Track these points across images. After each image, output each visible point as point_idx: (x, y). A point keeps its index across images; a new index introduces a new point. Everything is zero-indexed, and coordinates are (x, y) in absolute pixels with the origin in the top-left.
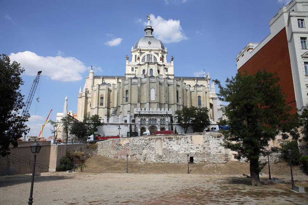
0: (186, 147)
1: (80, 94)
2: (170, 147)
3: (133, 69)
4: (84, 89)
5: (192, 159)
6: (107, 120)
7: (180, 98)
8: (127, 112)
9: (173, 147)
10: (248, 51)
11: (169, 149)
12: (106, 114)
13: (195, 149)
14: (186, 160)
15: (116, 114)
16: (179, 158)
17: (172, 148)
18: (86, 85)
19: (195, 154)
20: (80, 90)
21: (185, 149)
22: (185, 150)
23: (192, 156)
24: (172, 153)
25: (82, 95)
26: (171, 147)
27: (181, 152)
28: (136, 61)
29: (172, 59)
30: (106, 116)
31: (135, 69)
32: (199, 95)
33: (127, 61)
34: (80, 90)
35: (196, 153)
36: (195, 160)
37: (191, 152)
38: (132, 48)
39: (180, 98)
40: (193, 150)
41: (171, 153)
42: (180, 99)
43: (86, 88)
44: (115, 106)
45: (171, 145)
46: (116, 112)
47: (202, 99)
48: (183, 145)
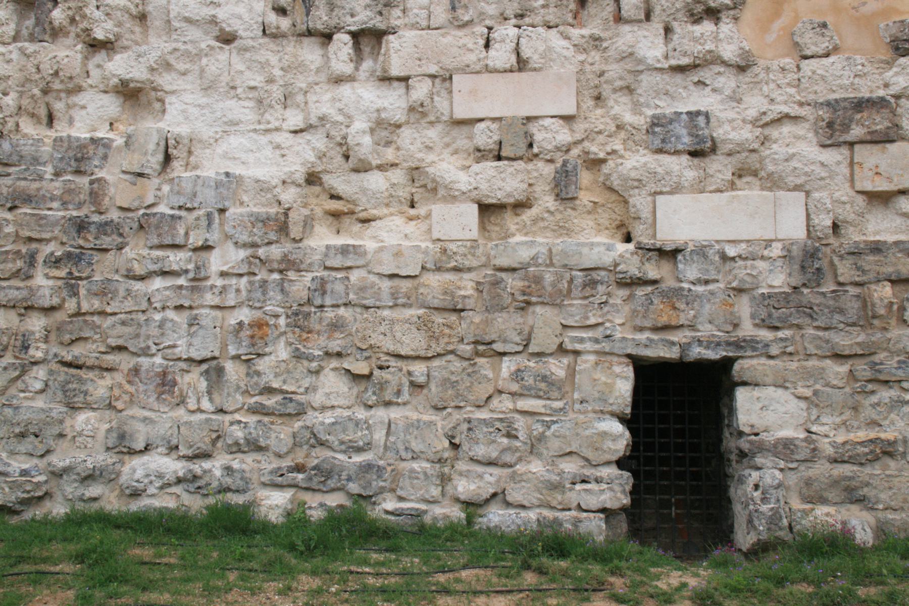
0: (547, 97)
2: (91, 116)
5: (681, 418)
9: (183, 113)
11: (79, 157)
13: (799, 148)
14: (573, 460)
16: (332, 386)
17: (151, 128)
19: (778, 280)
21: (512, 144)
22: (504, 181)
23: (696, 338)
24: (137, 254)
26: (131, 94)
27: (393, 238)
35: (809, 260)
36: (785, 449)
37: (682, 219)
40: (719, 168)
41: (104, 268)
45: (119, 66)
48: (461, 46)
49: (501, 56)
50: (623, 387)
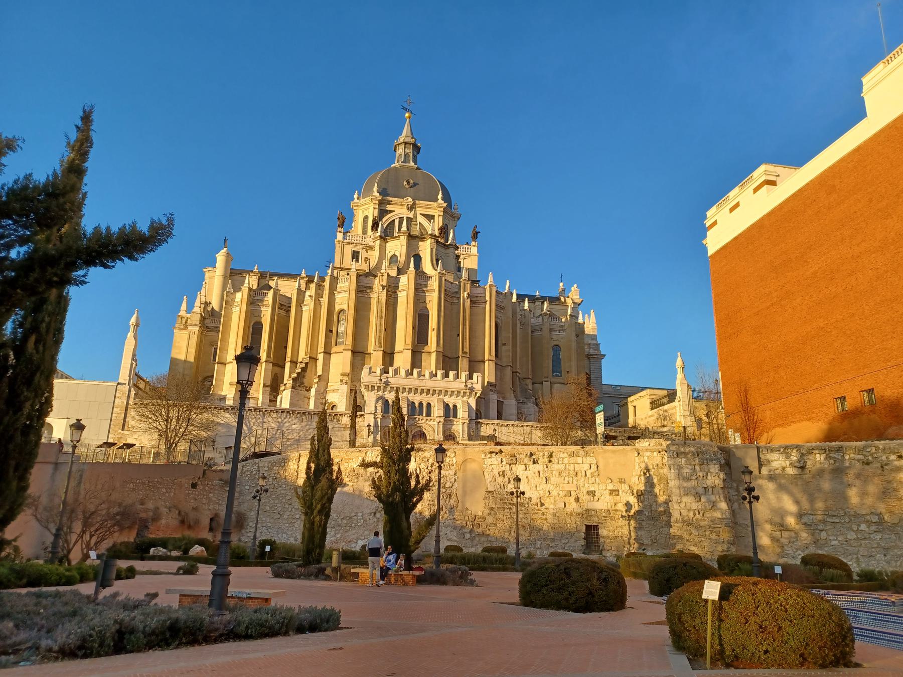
1: (182, 317)
3: (355, 256)
4: (197, 303)
6: (270, 401)
7: (505, 344)
8: (340, 377)
10: (756, 190)
12: (269, 383)
15: (302, 383)
18: (203, 290)
20: (184, 306)
25: (189, 322)
28: (365, 232)
29: (475, 236)
30: (269, 389)
31: (363, 255)
32: (555, 343)
33: (339, 229)
34: (184, 306)
38: (356, 196)
39: (505, 344)
42: (504, 348)
43: (203, 300)
44: (302, 356)
46: (304, 377)
47: (563, 355)
49: (566, 482)
50: (584, 528)
